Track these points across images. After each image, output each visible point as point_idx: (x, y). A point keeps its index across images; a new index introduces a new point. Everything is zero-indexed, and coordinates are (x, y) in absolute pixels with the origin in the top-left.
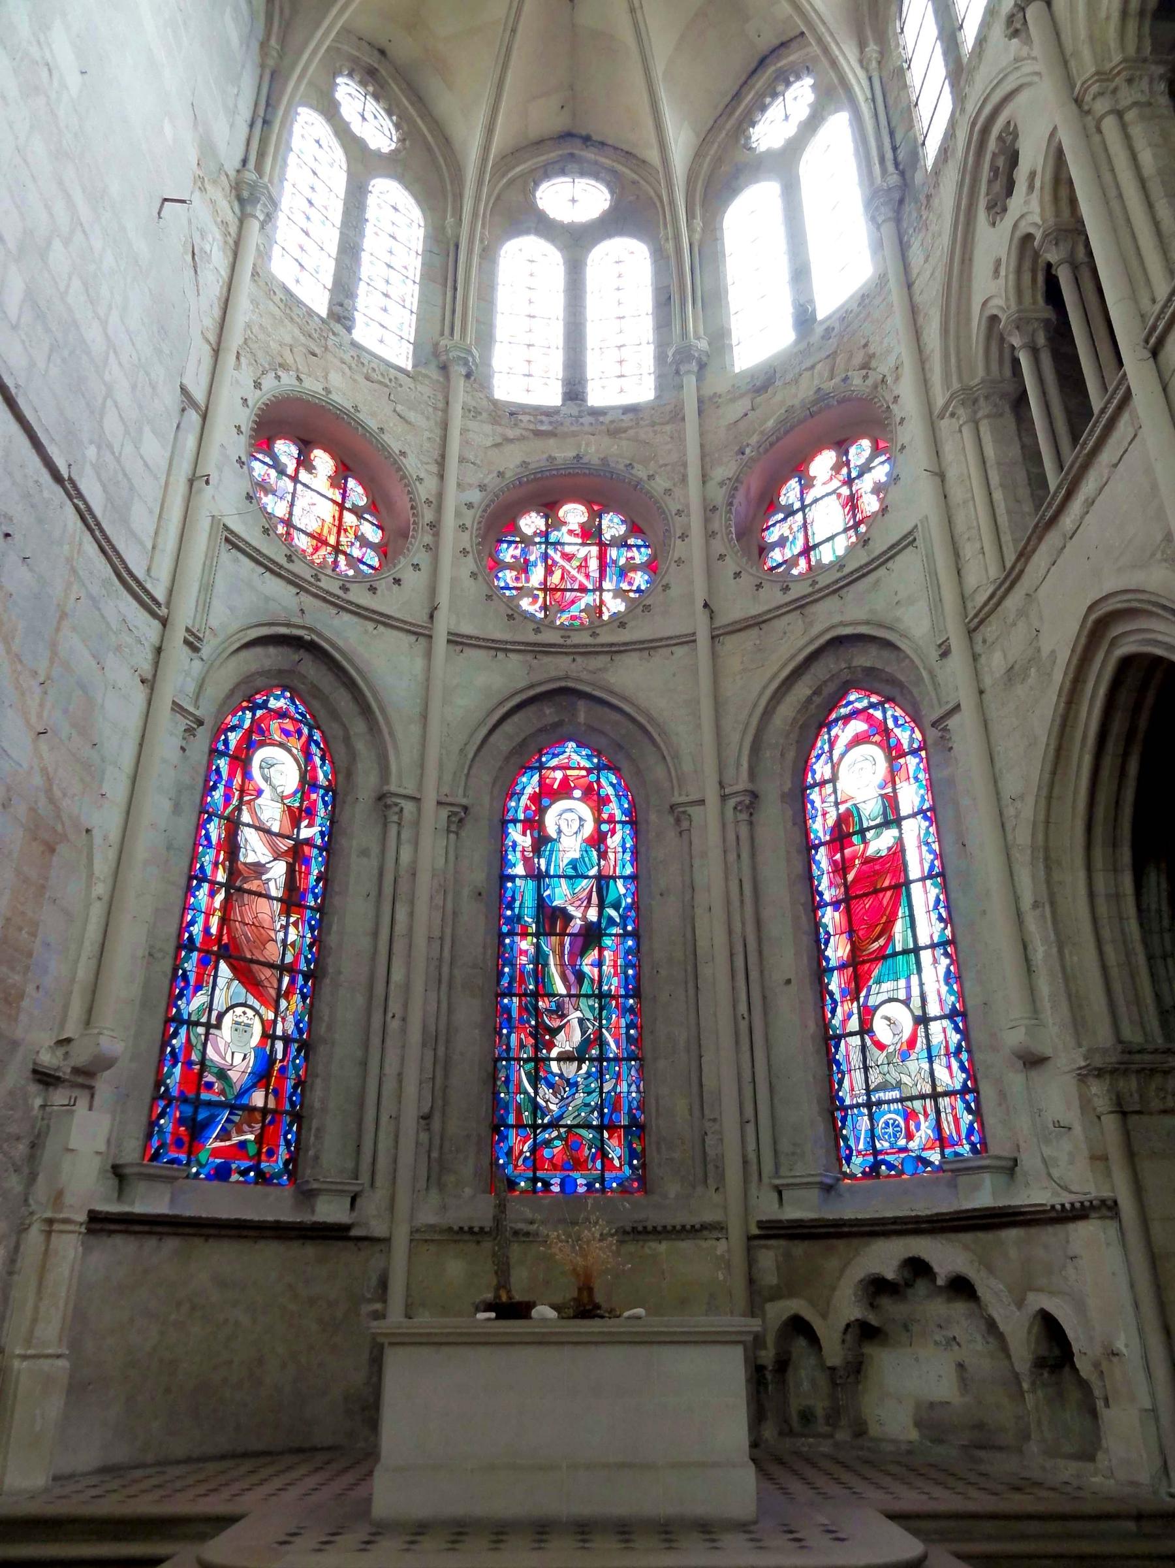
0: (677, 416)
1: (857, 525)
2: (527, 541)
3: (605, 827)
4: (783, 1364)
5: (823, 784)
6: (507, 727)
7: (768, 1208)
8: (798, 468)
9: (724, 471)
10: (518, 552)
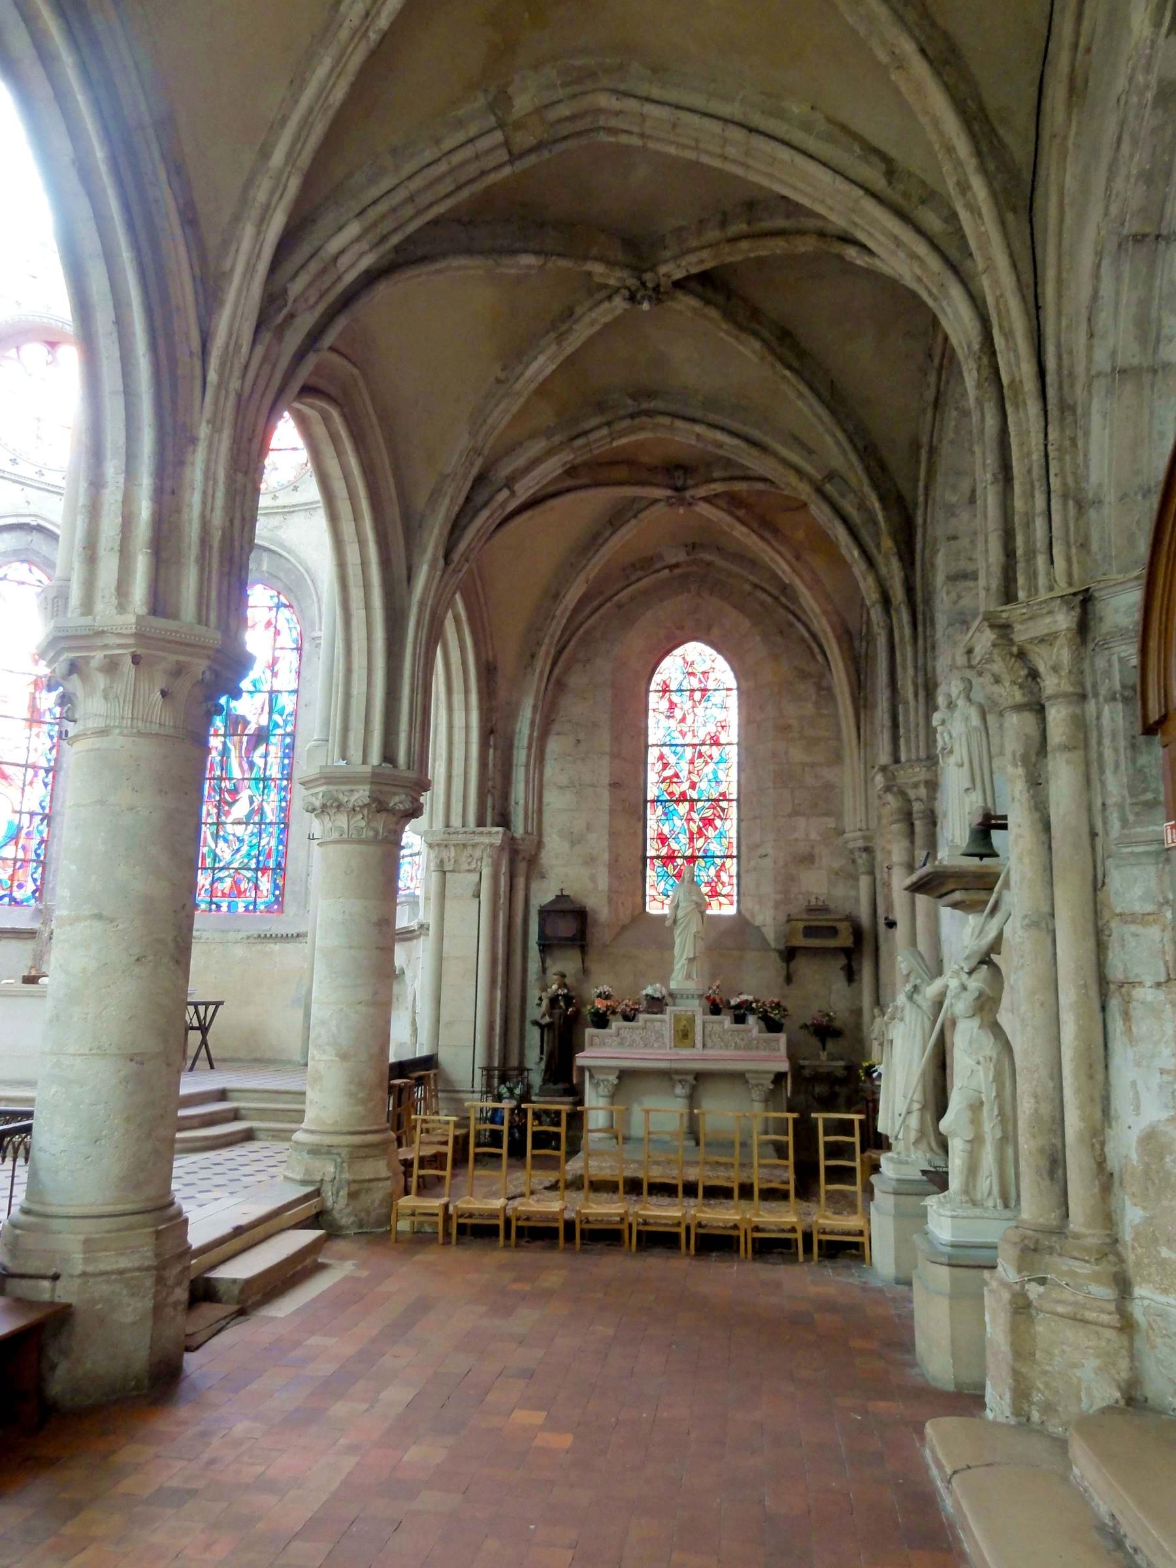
3: (278, 653)
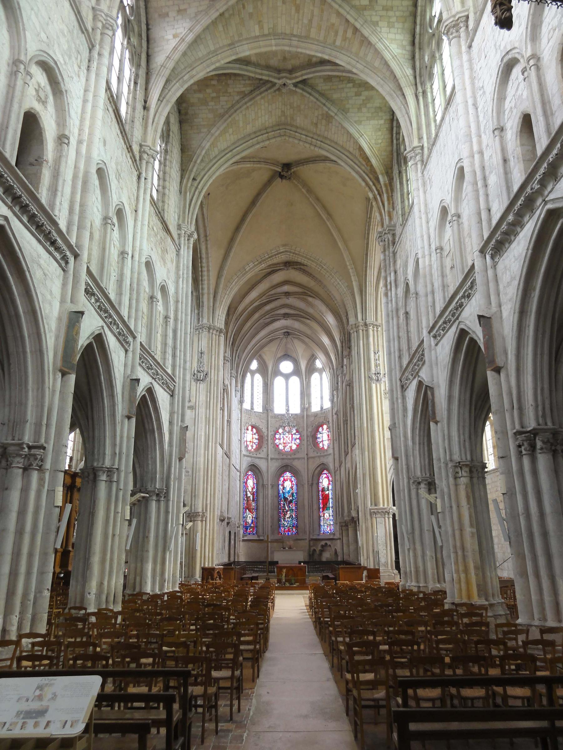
0: (303, 417)
4: (313, 554)
7: (312, 537)
8: (322, 426)
9: (310, 430)
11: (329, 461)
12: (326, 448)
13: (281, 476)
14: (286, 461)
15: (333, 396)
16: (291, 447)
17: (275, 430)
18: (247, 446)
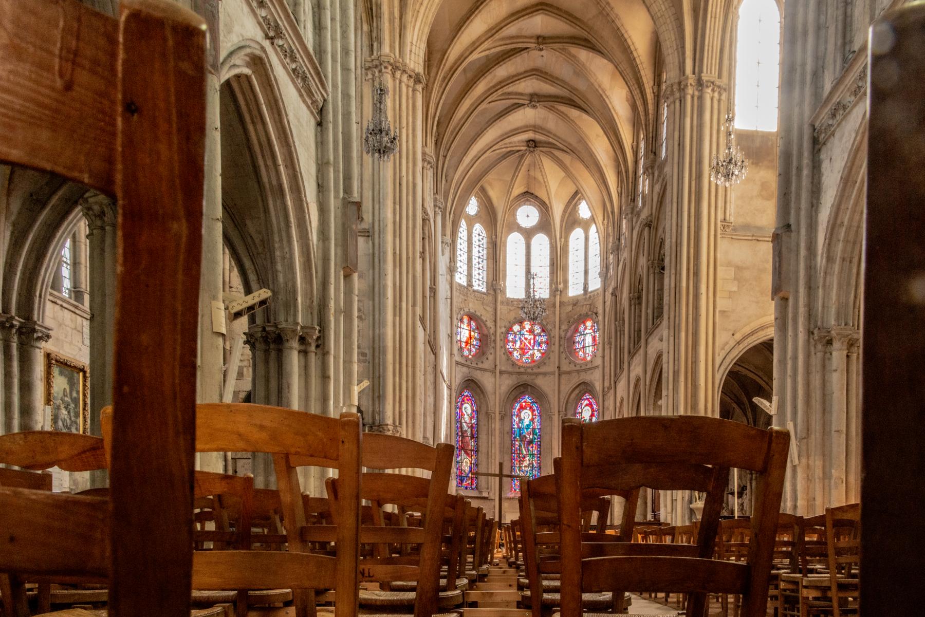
0: (554, 306)
1: (594, 345)
2: (515, 334)
5: (579, 413)
6: (513, 393)
8: (584, 323)
10: (513, 337)
11: (596, 378)
12: (589, 358)
13: (516, 399)
14: (525, 377)
15: (607, 268)
16: (532, 355)
17: (507, 325)
18: (461, 349)
